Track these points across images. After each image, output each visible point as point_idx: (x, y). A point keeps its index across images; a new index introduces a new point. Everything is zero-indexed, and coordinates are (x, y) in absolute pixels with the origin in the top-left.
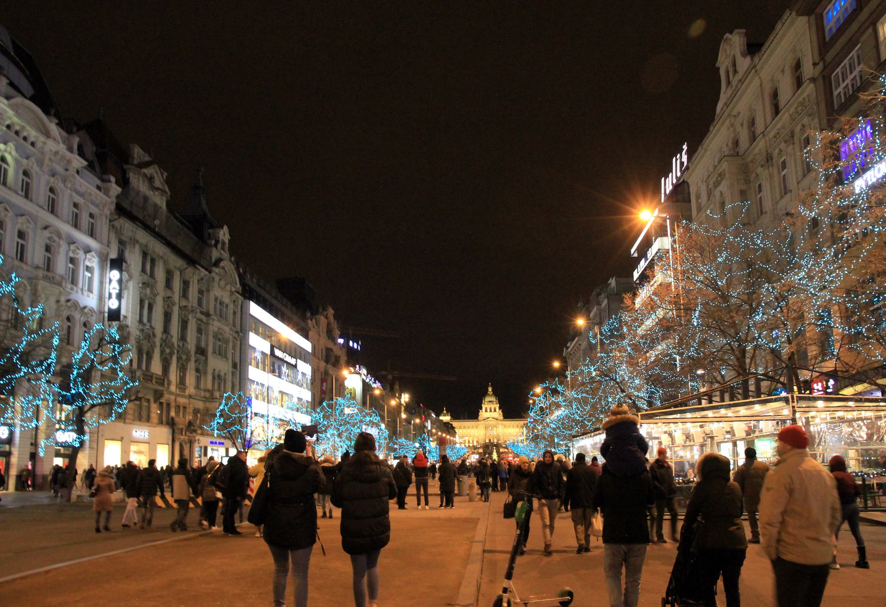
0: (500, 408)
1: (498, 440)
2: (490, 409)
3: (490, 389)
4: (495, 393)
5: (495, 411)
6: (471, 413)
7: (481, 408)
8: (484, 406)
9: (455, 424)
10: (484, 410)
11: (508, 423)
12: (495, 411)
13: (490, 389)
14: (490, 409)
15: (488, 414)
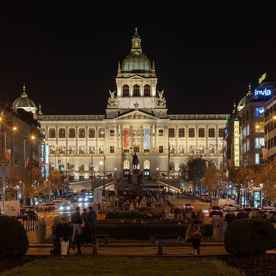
0: (158, 89)
1: (154, 164)
2: (136, 91)
3: (136, 42)
4: (148, 52)
5: (147, 94)
6: (90, 99)
7: (115, 89)
8: (120, 83)
9: (47, 125)
10: (120, 92)
11: (178, 124)
12: (147, 94)
13: (136, 42)
14: (136, 91)
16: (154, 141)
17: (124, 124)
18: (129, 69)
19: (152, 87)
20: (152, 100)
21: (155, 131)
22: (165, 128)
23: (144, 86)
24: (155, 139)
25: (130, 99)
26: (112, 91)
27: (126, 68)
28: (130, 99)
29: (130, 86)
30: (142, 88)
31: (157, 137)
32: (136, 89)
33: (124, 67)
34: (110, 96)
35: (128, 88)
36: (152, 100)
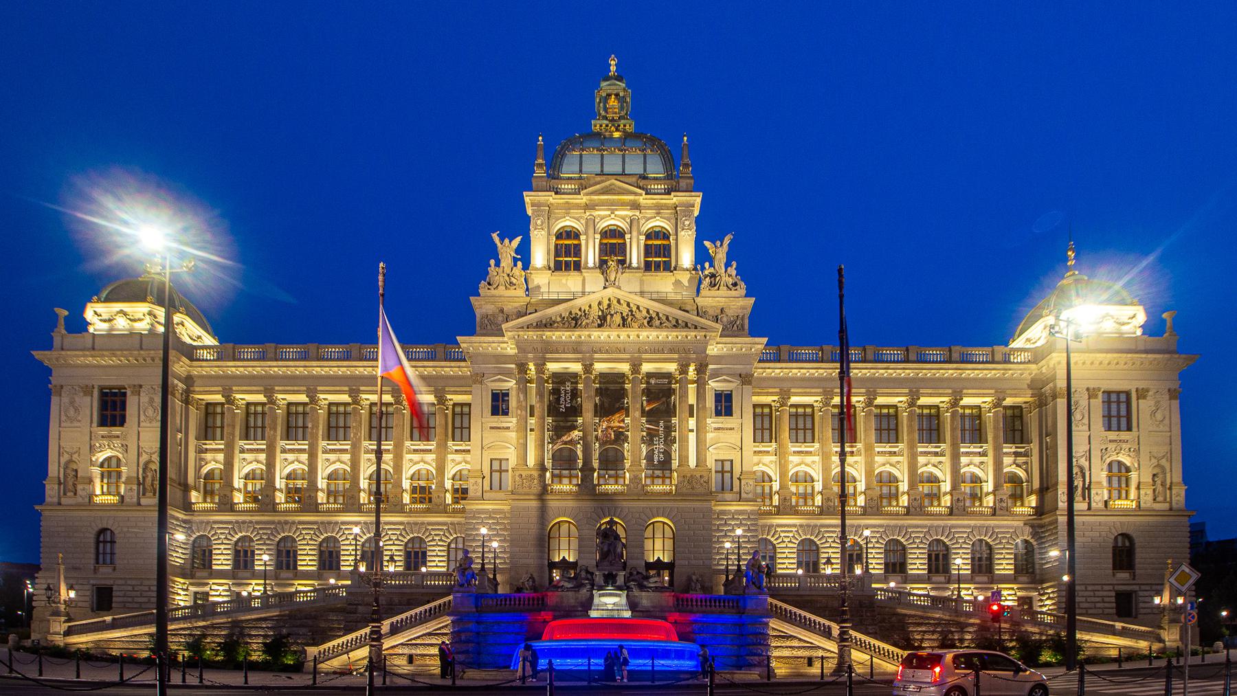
3: (612, 95)
10: (540, 255)
13: (612, 95)
15: (586, 288)
16: (692, 437)
17: (557, 356)
18: (581, 171)
19: (682, 234)
20: (678, 283)
21: (700, 395)
22: (743, 383)
23: (645, 229)
24: (700, 430)
25: (584, 280)
26: (507, 235)
27: (569, 168)
28: (584, 280)
29: (586, 229)
30: (635, 234)
31: (709, 421)
32: (606, 256)
33: (561, 164)
34: (495, 255)
35: (576, 242)
36: (678, 283)
